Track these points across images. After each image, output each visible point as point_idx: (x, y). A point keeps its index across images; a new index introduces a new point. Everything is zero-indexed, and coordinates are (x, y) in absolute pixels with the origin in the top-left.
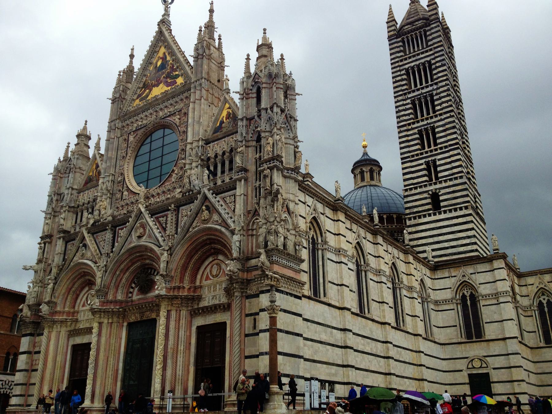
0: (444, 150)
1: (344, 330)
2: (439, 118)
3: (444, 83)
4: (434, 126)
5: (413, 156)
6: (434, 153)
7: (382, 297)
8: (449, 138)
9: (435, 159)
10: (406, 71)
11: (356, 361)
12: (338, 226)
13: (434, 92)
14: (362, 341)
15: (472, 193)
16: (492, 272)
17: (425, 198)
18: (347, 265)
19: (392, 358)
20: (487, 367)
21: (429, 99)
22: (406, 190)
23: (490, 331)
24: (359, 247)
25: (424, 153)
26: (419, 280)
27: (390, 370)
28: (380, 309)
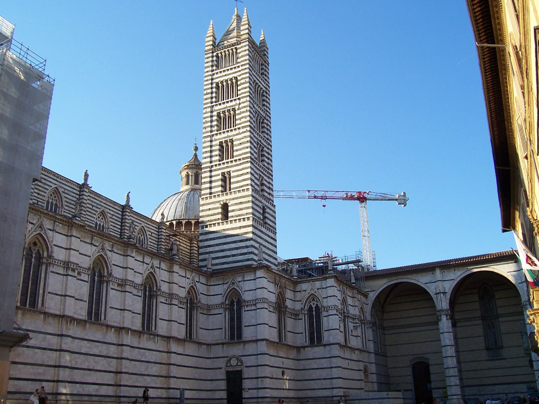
0: (238, 162)
1: (62, 335)
2: (237, 131)
3: (244, 100)
6: (230, 164)
7: (124, 306)
10: (216, 85)
11: (76, 362)
12: (71, 241)
14: (88, 345)
15: (260, 205)
16: (255, 281)
17: (217, 208)
18: (76, 277)
19: (127, 359)
20: (241, 365)
21: (232, 112)
23: (247, 333)
25: (222, 165)
26: (188, 287)
27: (121, 369)
28: (120, 315)
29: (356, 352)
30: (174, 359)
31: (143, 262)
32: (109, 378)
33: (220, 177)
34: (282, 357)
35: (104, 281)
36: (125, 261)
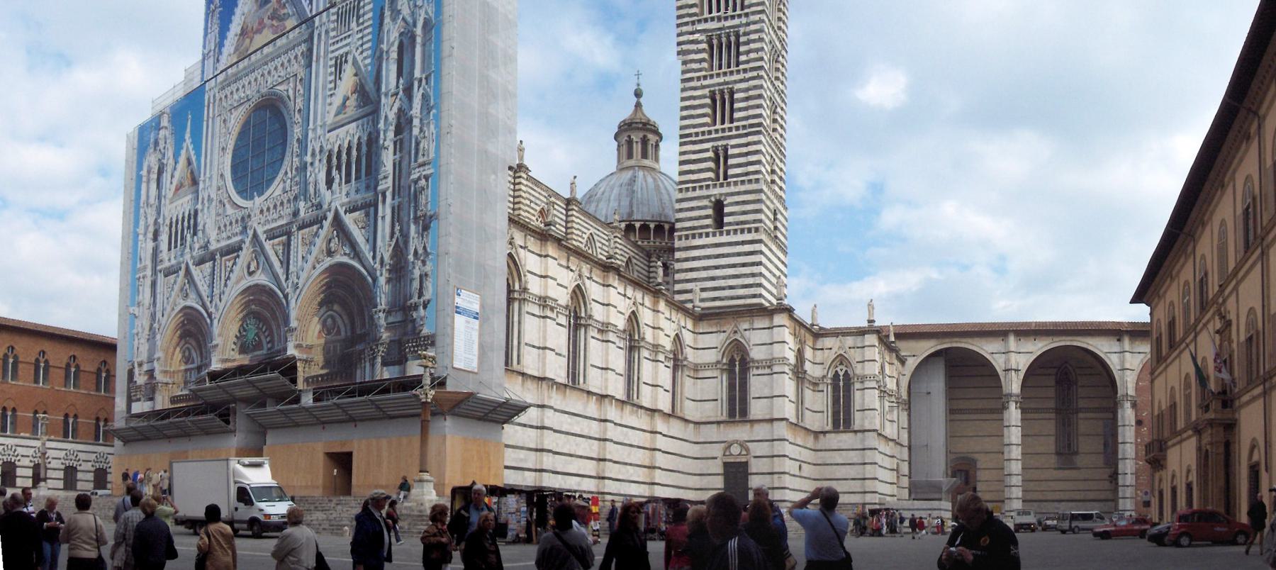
0: (741, 132)
2: (741, 76)
3: (757, 17)
4: (733, 88)
5: (697, 134)
8: (751, 112)
9: (728, 145)
11: (557, 444)
13: (742, 30)
14: (569, 420)
19: (611, 441)
21: (733, 39)
22: (681, 190)
24: (578, 293)
25: (713, 132)
27: (605, 455)
29: (891, 444)
30: (661, 442)
31: (625, 295)
32: (590, 468)
33: (711, 154)
34: (799, 446)
35: (581, 325)
36: (605, 294)
